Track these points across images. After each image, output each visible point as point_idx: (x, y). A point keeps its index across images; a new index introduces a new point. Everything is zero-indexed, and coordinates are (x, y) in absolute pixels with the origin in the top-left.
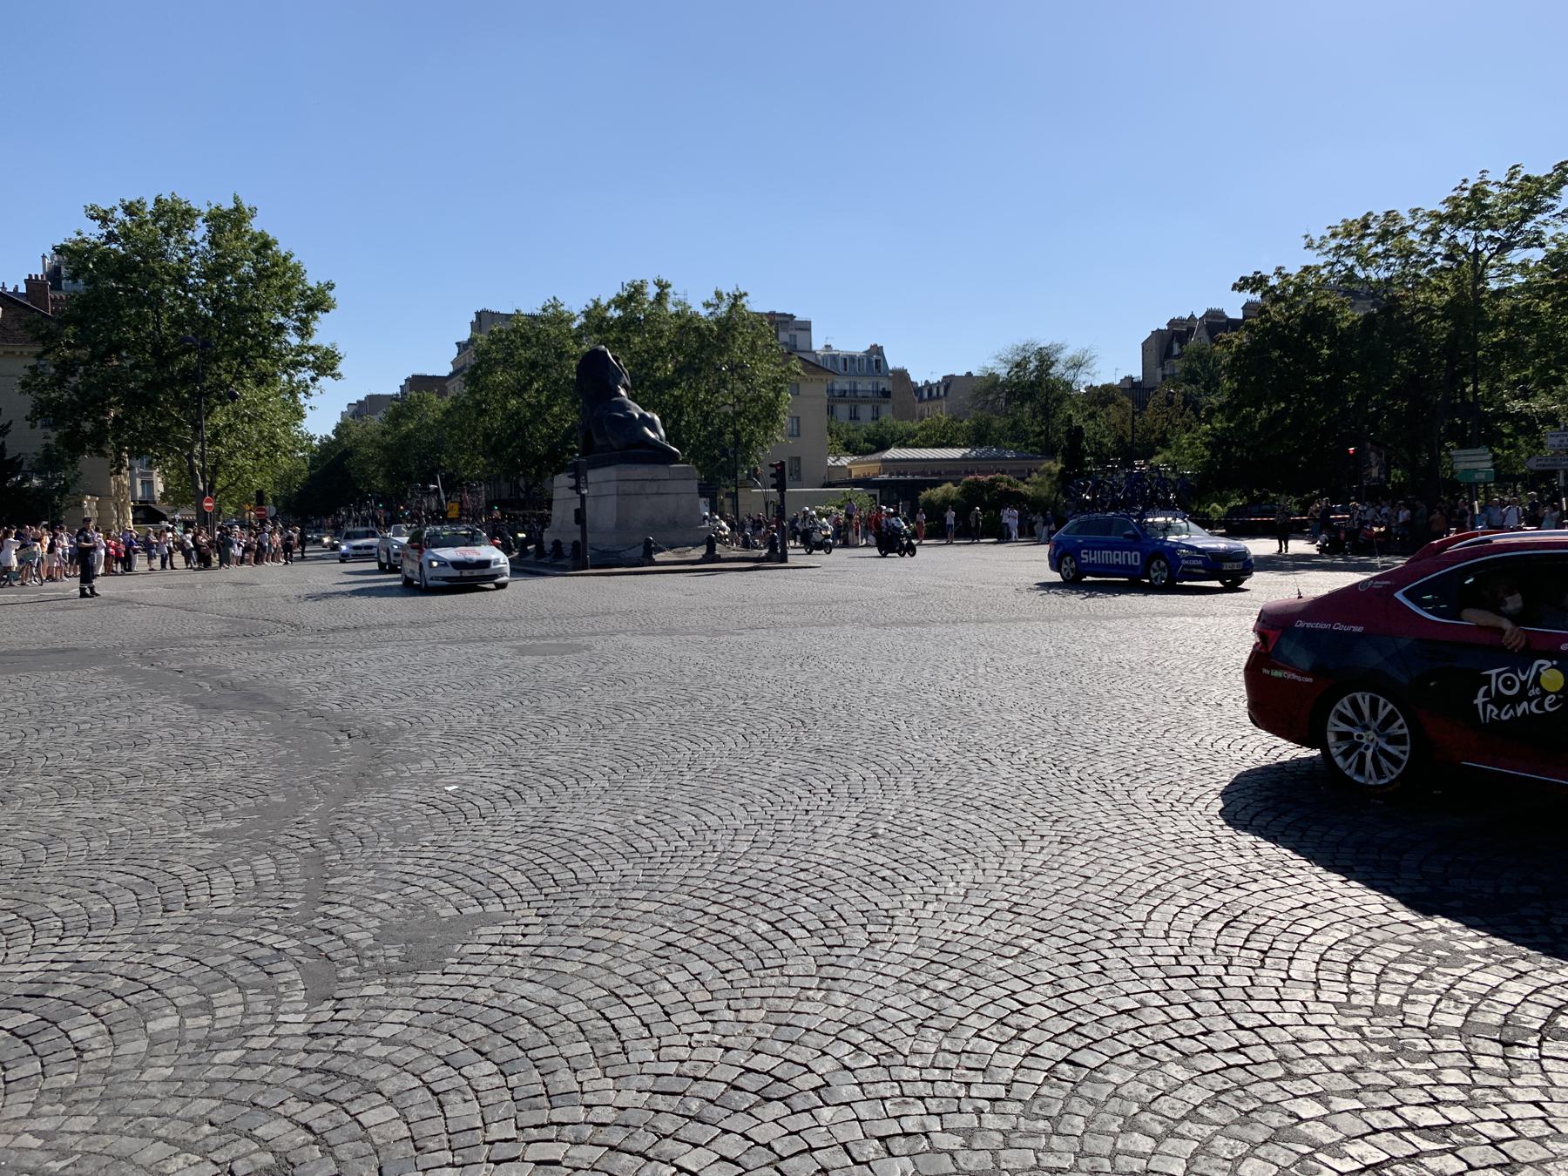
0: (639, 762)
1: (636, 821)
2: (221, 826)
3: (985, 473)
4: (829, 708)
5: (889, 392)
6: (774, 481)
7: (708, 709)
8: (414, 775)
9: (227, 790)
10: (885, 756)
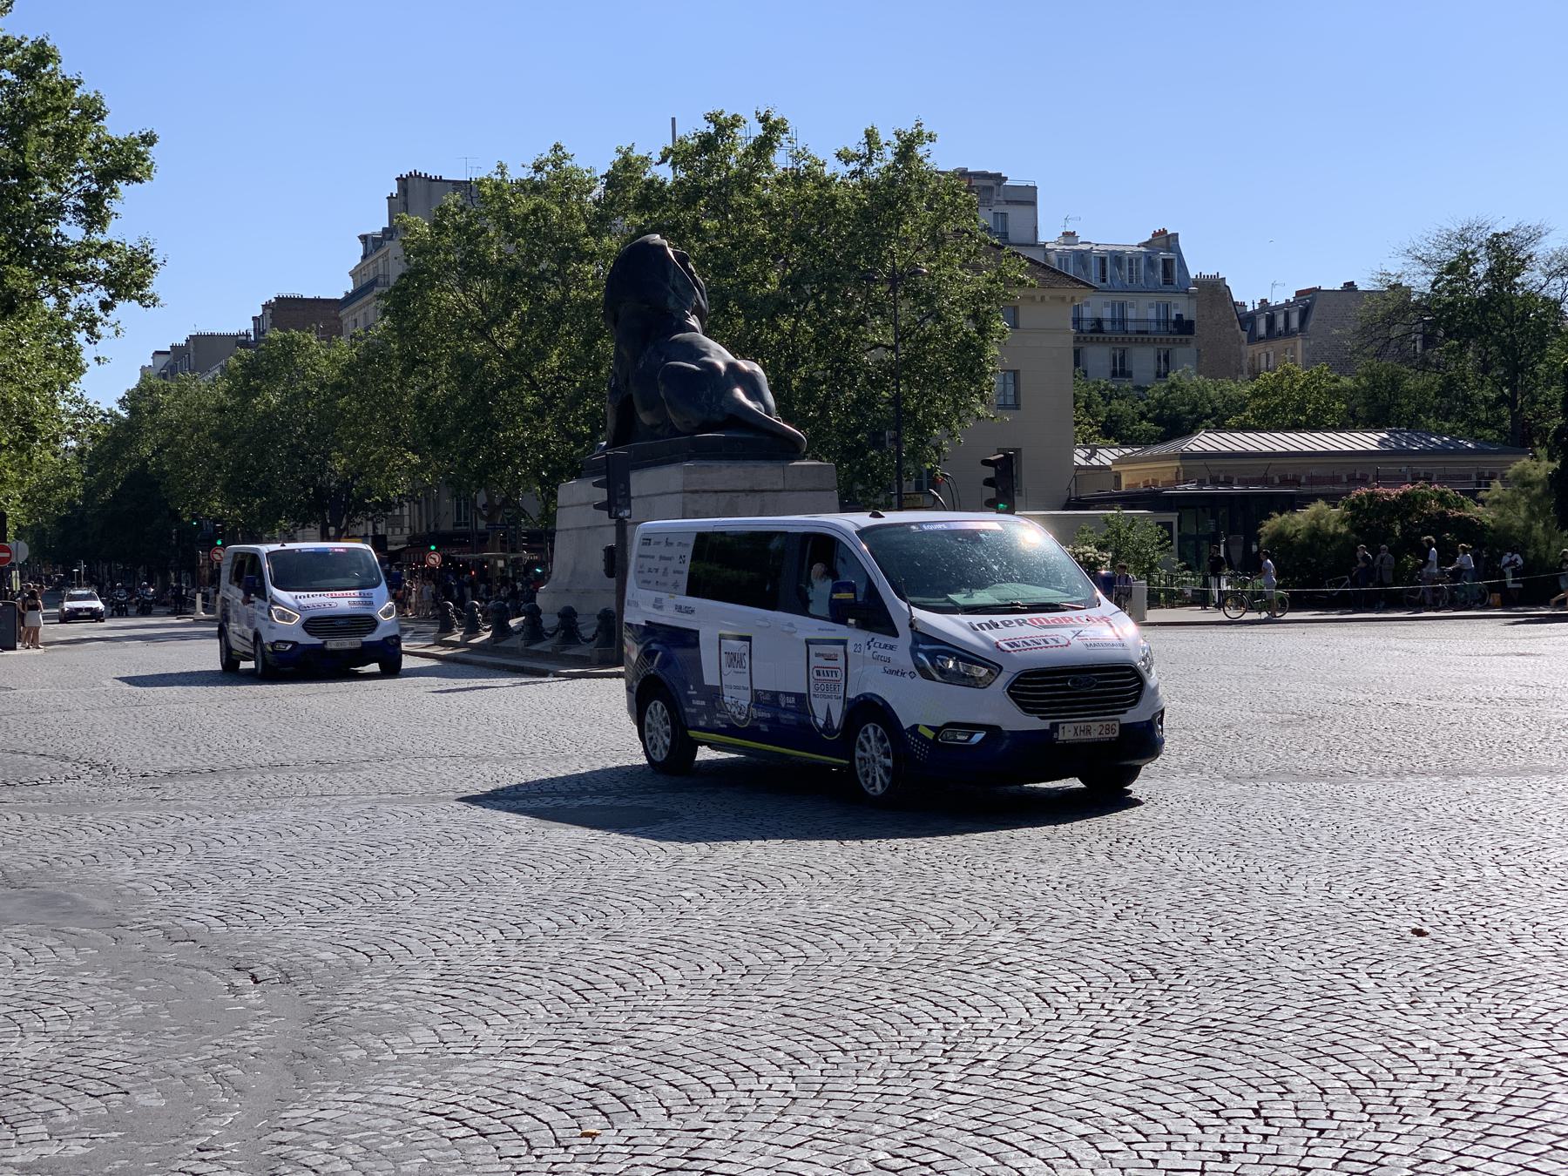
0: (842, 1041)
1: (875, 1163)
2: (52, 1151)
3: (1399, 480)
4: (1197, 942)
5: (1191, 323)
6: (991, 493)
7: (949, 939)
8: (401, 1057)
9: (46, 1082)
10: (1351, 1043)
